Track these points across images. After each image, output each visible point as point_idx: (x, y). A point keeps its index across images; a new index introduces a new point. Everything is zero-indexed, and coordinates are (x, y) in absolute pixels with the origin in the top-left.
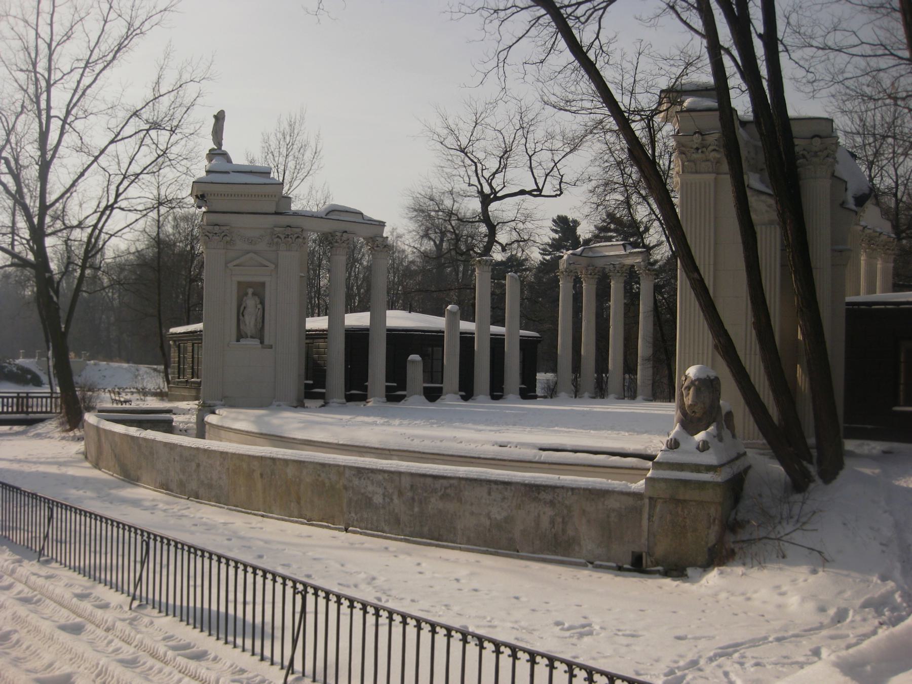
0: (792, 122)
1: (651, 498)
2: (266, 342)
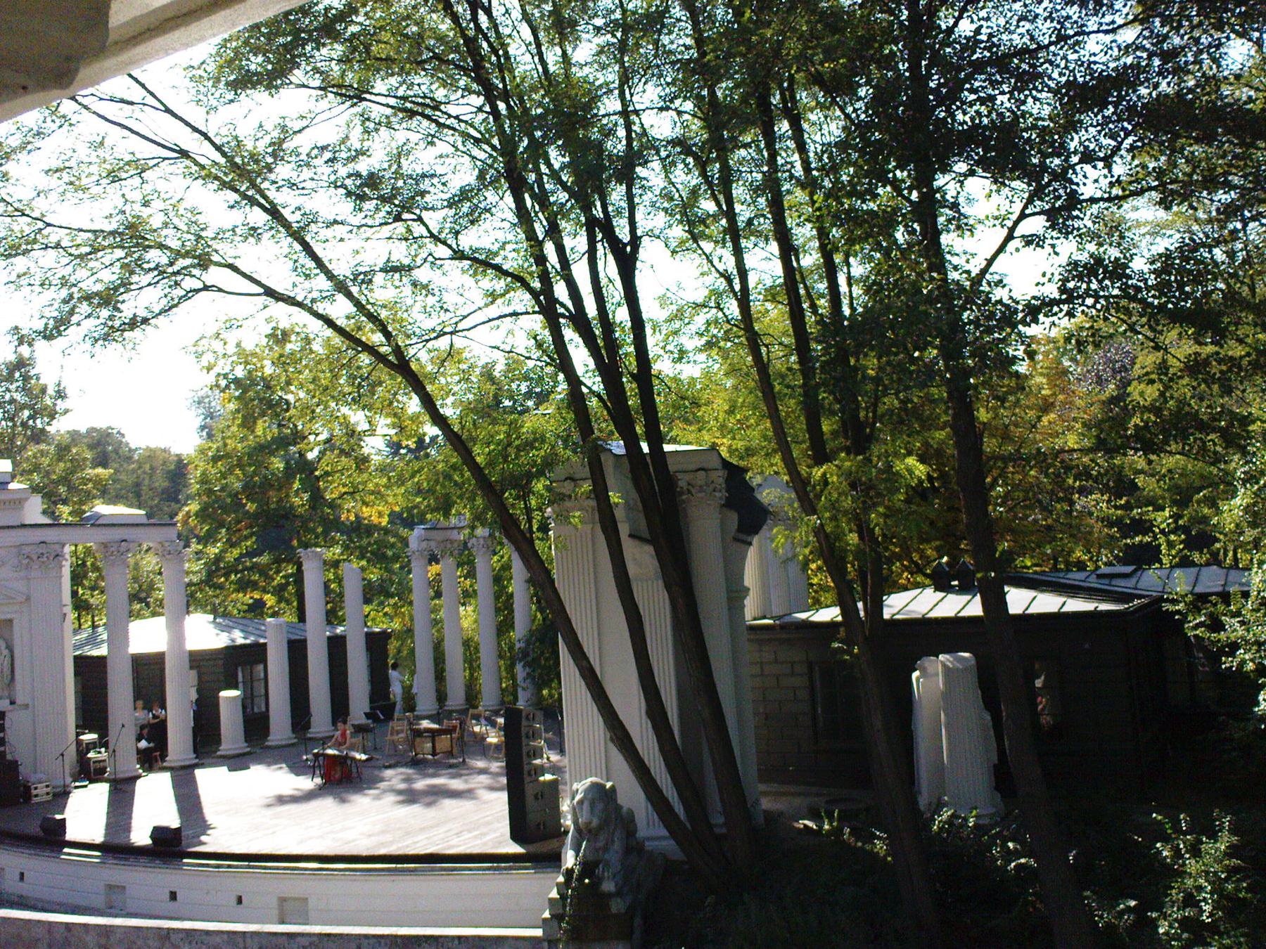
0: (669, 461)
1: (550, 942)
2: (20, 699)
